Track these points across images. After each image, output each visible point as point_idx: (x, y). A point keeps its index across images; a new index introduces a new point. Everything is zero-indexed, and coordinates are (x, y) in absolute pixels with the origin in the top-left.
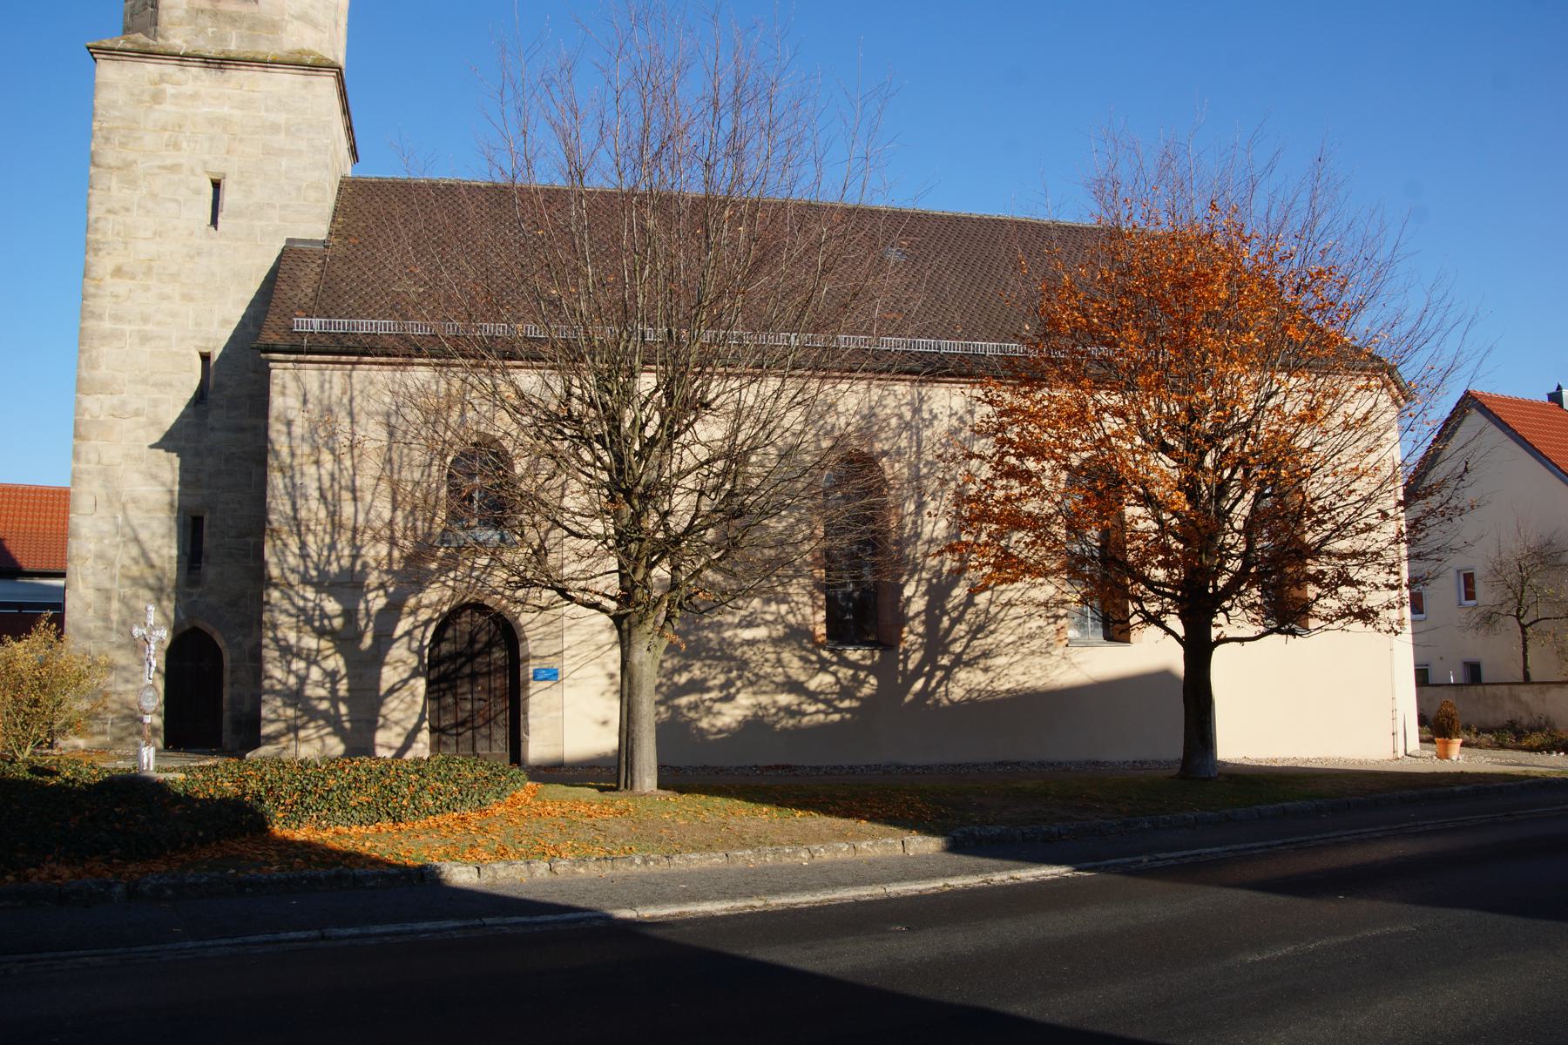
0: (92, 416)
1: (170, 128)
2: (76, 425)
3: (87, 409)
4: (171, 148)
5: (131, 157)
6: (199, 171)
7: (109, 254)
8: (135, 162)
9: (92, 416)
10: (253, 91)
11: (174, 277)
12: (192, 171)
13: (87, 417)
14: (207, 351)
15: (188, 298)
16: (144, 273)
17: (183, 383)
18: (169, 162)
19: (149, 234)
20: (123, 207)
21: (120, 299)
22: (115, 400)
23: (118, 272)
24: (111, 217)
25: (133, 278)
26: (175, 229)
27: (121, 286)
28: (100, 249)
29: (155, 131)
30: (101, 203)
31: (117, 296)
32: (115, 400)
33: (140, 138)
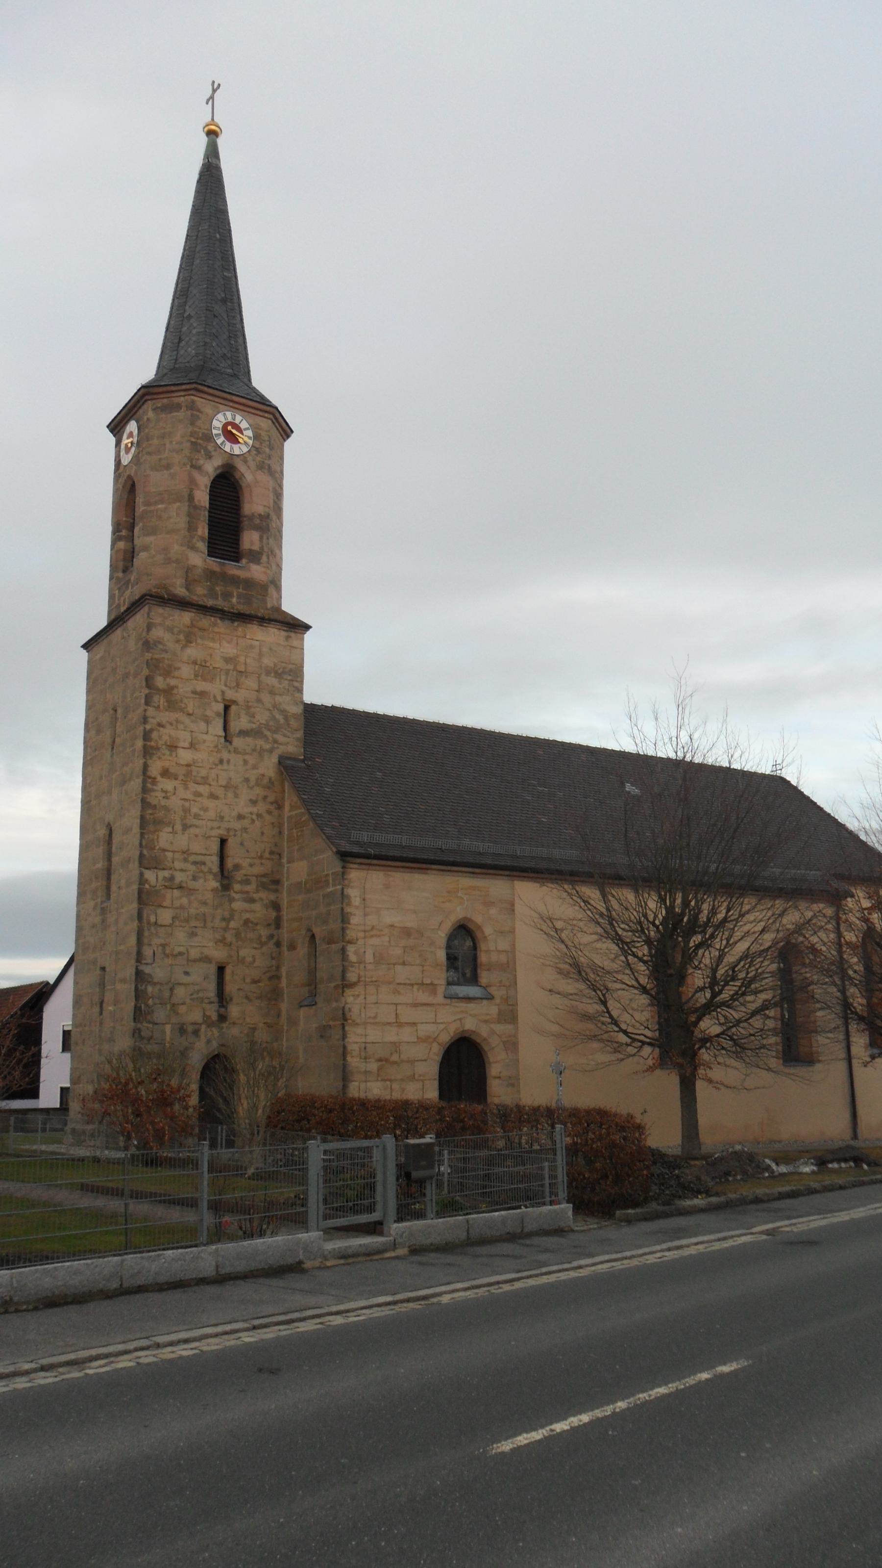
0: (150, 886)
1: (199, 662)
2: (140, 892)
3: (147, 880)
4: (200, 678)
5: (173, 682)
6: (219, 698)
7: (160, 758)
8: (177, 687)
9: (150, 886)
10: (252, 639)
11: (205, 781)
12: (215, 697)
13: (147, 886)
14: (225, 838)
15: (213, 796)
16: (184, 775)
17: (212, 862)
18: (199, 689)
19: (187, 745)
20: (168, 722)
21: (168, 794)
22: (166, 874)
23: (165, 773)
24: (161, 729)
25: (176, 779)
26: (204, 741)
27: (167, 784)
28: (153, 754)
29: (188, 663)
30: (153, 718)
31: (166, 792)
32: (166, 874)
33: (179, 668)
